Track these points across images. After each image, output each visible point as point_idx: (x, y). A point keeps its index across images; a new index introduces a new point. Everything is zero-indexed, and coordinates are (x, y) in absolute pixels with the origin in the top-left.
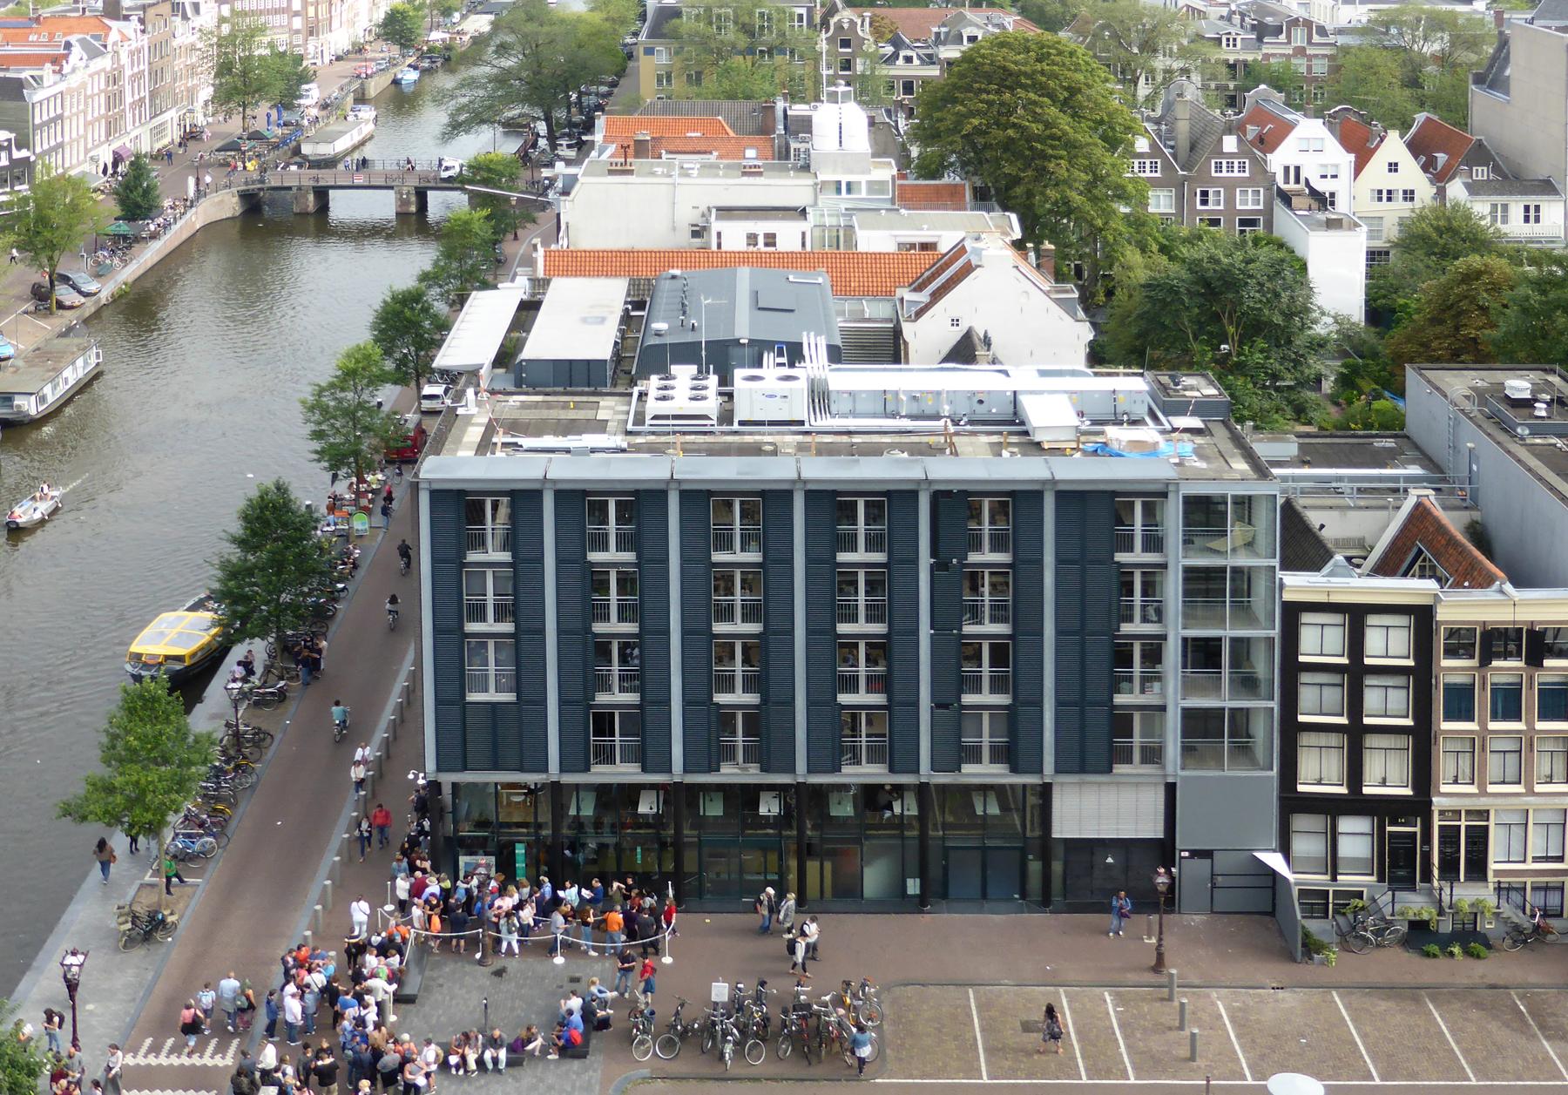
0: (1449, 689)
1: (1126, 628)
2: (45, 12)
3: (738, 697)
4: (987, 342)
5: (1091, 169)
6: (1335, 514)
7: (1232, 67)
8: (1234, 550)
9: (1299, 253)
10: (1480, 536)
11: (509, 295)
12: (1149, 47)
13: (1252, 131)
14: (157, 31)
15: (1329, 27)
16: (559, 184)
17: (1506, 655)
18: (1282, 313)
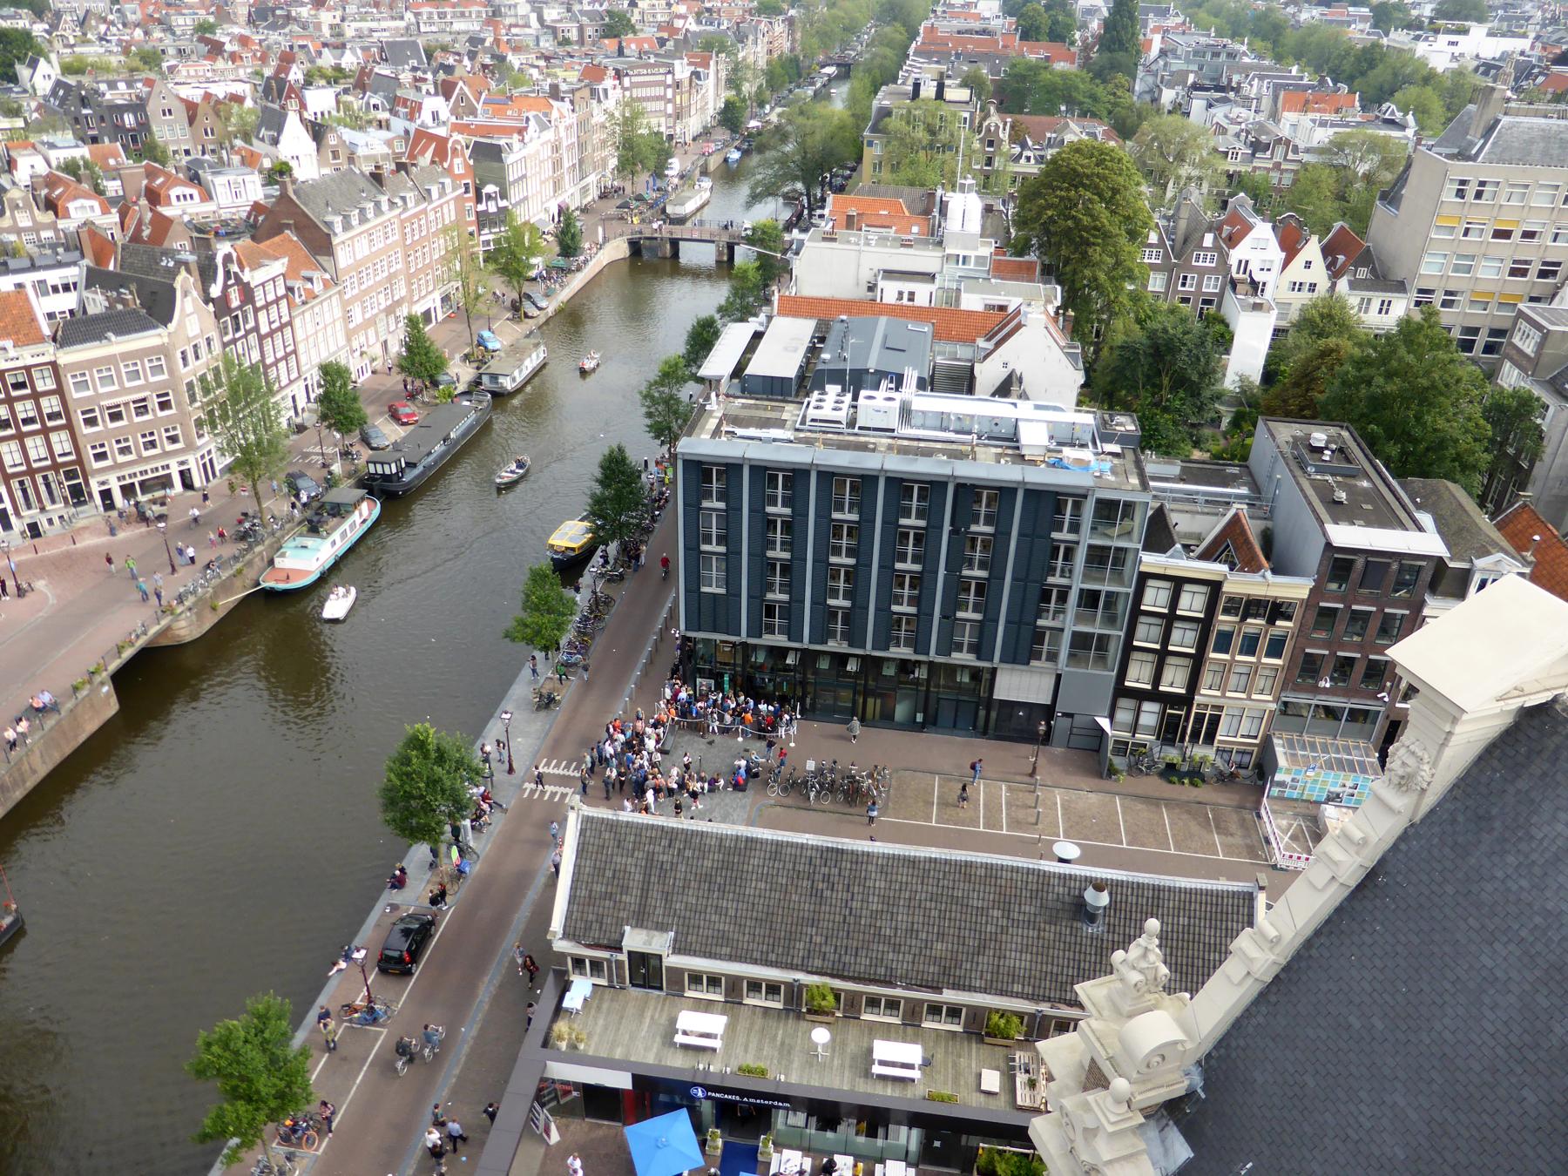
0: (1220, 633)
1: (1051, 580)
2: (516, 93)
3: (840, 602)
4: (1020, 381)
5: (1115, 255)
6: (1188, 515)
7: (1230, 177)
8: (1118, 536)
9: (1231, 328)
10: (1268, 539)
11: (753, 325)
12: (1180, 158)
13: (1227, 229)
14: (582, 111)
15: (1302, 146)
16: (794, 247)
17: (1255, 616)
18: (1199, 373)
